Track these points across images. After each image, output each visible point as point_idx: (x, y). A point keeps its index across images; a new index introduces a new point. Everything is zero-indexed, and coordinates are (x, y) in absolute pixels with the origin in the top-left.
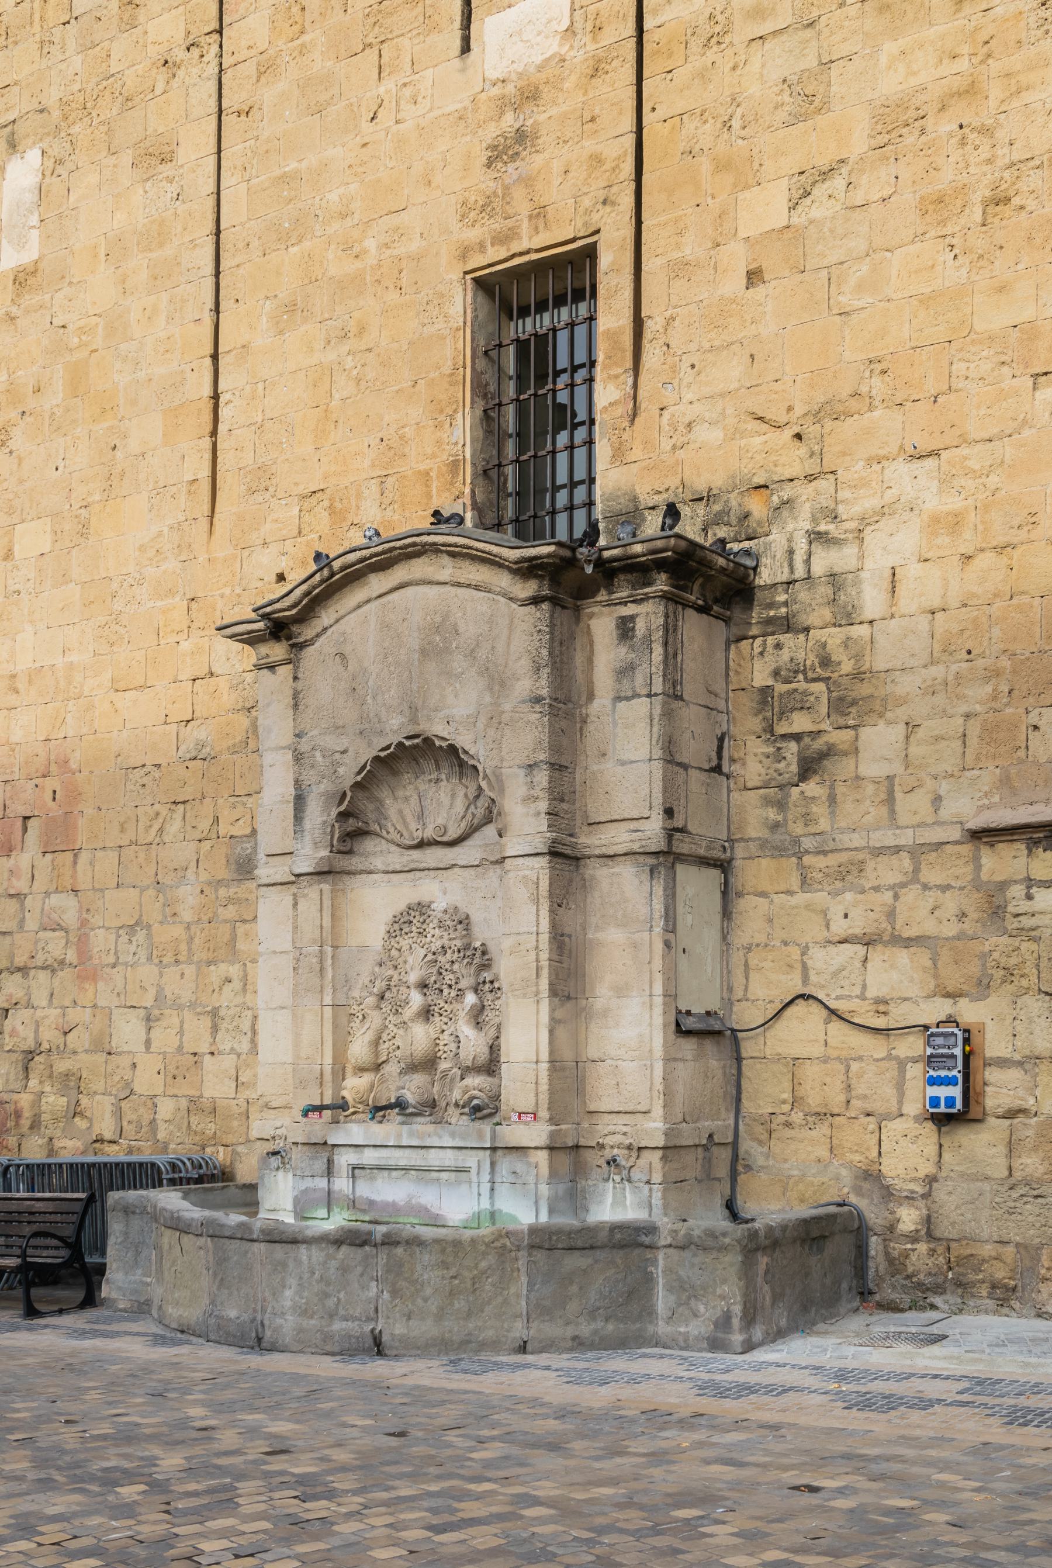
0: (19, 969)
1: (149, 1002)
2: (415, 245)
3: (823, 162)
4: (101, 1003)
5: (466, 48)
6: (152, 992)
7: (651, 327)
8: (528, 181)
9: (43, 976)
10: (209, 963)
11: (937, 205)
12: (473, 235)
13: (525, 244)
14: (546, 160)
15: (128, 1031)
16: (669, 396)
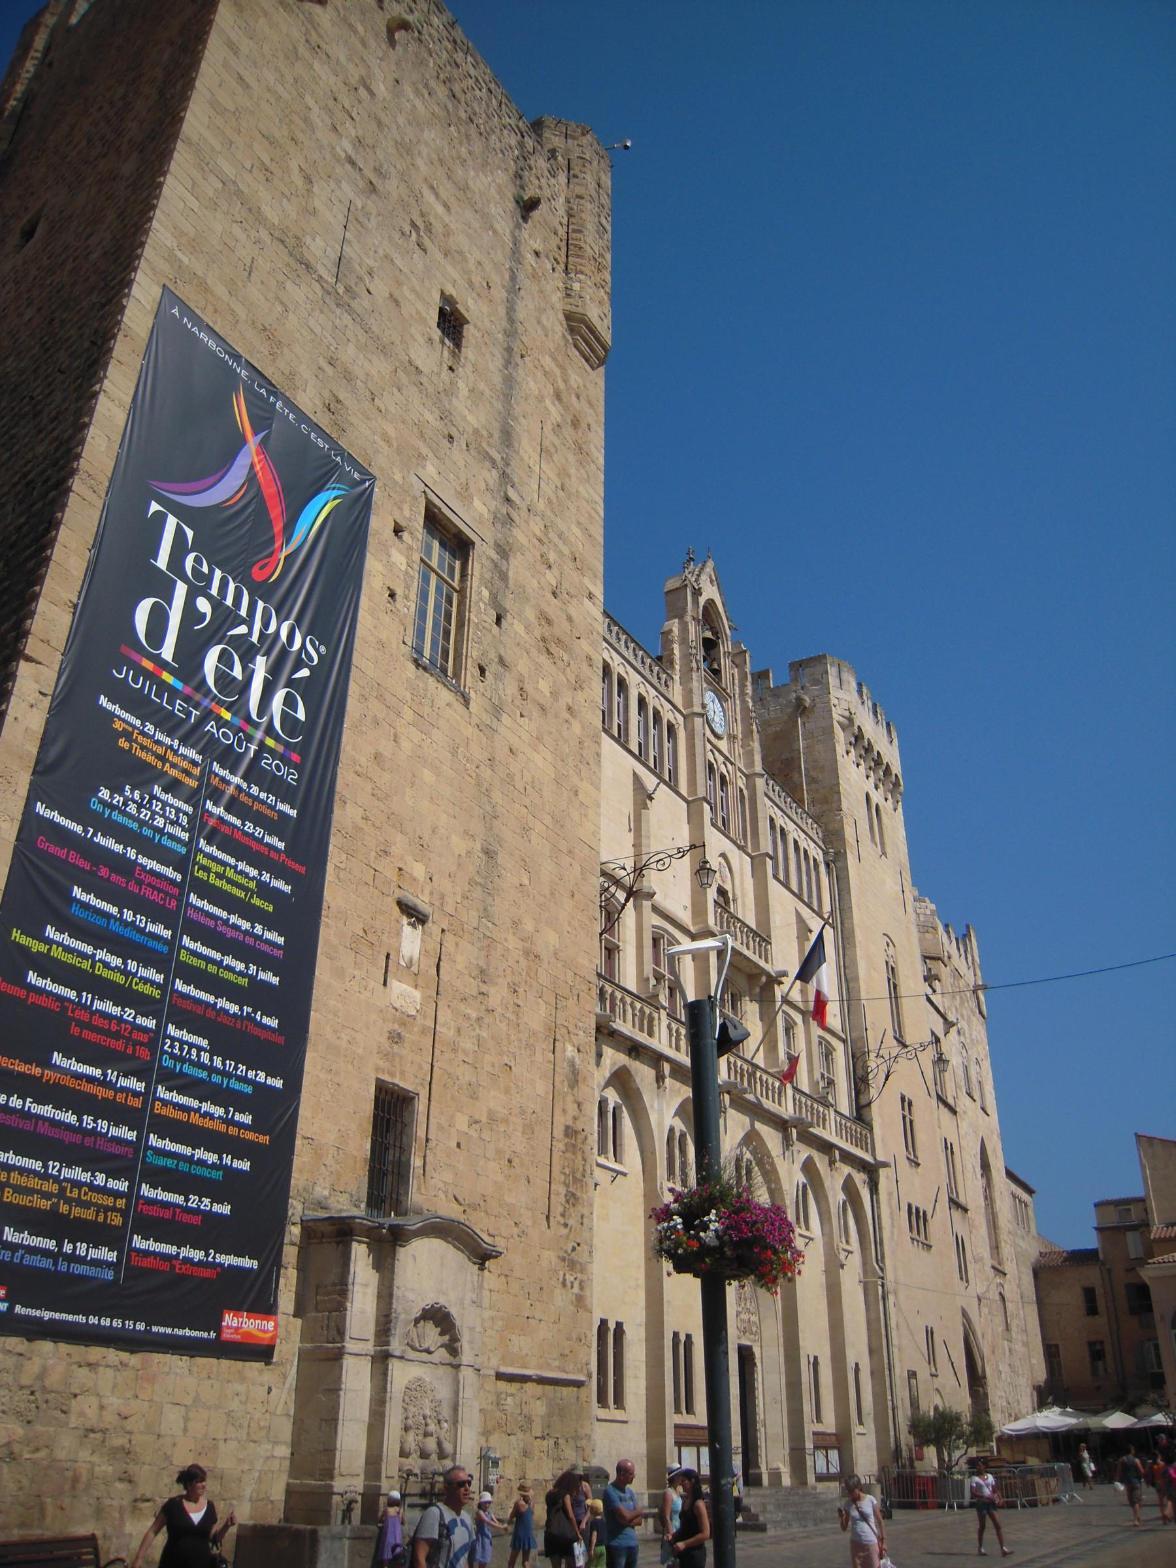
0: (89, 1365)
1: (188, 1401)
2: (360, 1051)
3: (477, 1117)
4: (156, 1399)
5: (385, 984)
6: (193, 1394)
7: (431, 1144)
8: (401, 1057)
9: (110, 1372)
10: (229, 1381)
11: (499, 1151)
12: (381, 1063)
13: (396, 1081)
14: (404, 1051)
15: (172, 1419)
16: (435, 1175)
